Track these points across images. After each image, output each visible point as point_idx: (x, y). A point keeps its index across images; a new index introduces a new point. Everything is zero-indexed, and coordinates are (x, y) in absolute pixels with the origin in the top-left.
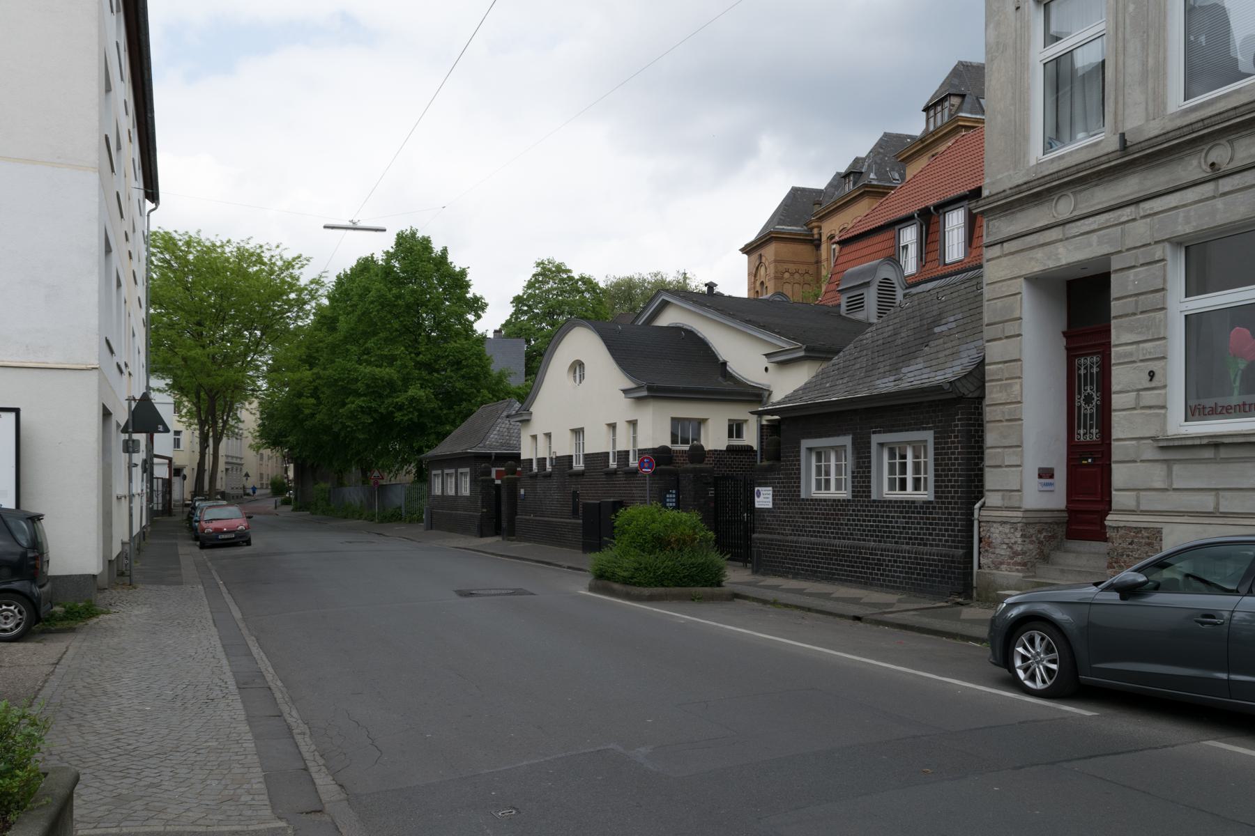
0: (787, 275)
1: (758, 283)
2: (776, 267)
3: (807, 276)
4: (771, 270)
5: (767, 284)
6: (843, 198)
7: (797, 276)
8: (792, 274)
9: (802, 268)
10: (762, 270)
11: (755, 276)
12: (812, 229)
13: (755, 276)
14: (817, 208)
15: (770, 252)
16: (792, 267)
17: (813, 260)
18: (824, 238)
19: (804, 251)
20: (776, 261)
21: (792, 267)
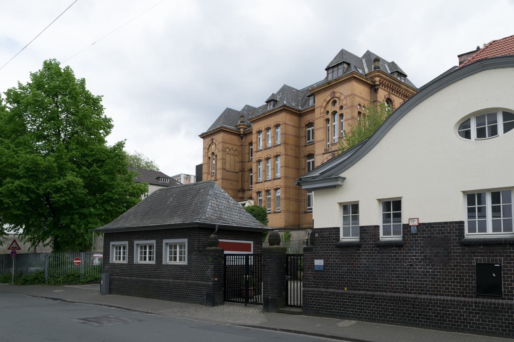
0: (227, 150)
1: (210, 153)
2: (223, 146)
3: (236, 152)
4: (220, 146)
5: (216, 153)
6: (269, 112)
7: (232, 151)
8: (230, 150)
9: (235, 148)
10: (213, 147)
11: (208, 149)
12: (239, 129)
13: (208, 149)
14: (242, 119)
15: (219, 137)
16: (230, 146)
17: (239, 144)
18: (254, 132)
19: (235, 139)
20: (223, 142)
21: (230, 146)
